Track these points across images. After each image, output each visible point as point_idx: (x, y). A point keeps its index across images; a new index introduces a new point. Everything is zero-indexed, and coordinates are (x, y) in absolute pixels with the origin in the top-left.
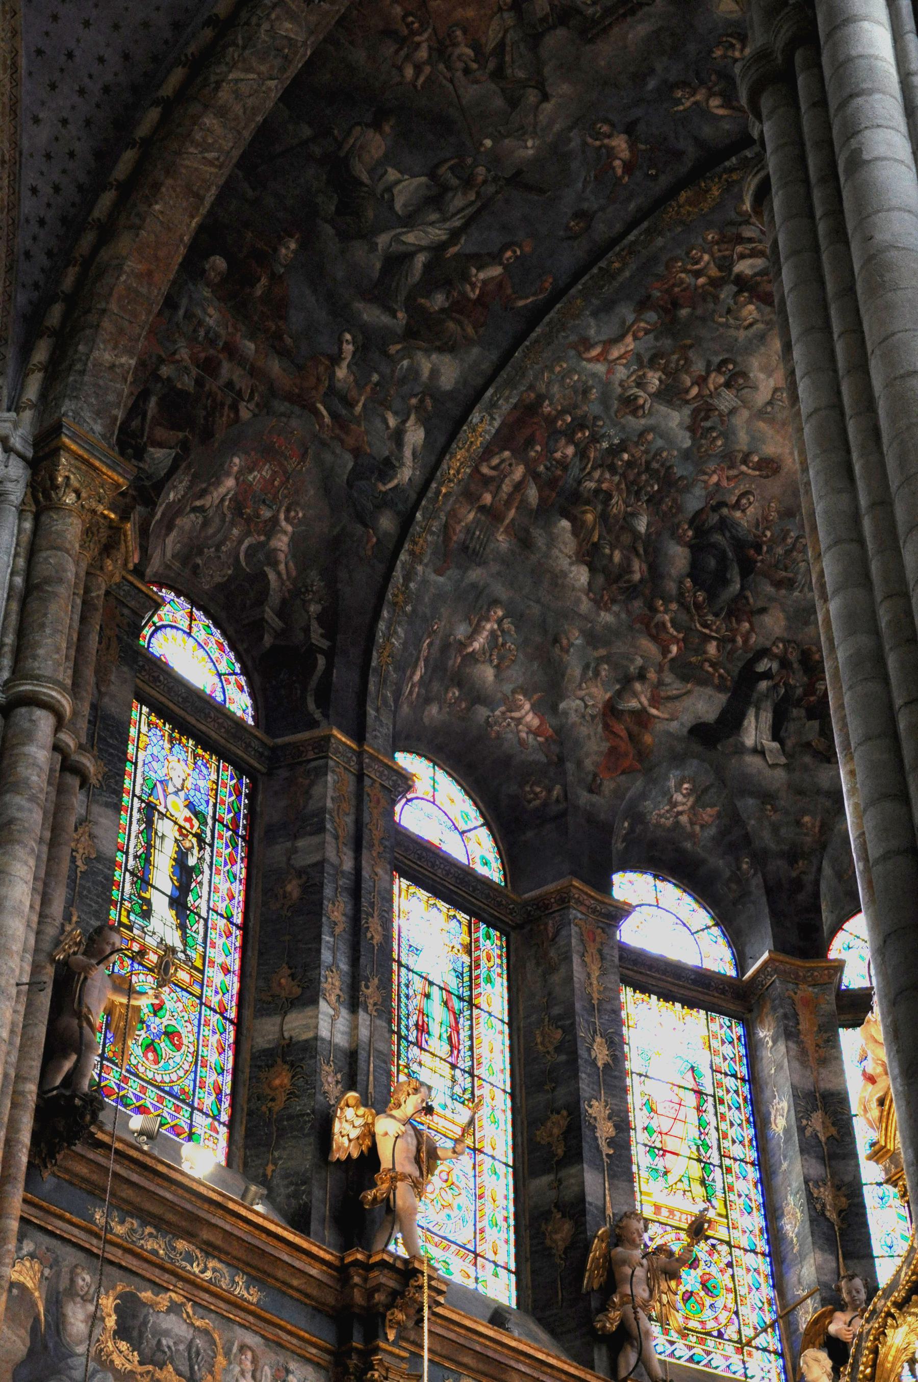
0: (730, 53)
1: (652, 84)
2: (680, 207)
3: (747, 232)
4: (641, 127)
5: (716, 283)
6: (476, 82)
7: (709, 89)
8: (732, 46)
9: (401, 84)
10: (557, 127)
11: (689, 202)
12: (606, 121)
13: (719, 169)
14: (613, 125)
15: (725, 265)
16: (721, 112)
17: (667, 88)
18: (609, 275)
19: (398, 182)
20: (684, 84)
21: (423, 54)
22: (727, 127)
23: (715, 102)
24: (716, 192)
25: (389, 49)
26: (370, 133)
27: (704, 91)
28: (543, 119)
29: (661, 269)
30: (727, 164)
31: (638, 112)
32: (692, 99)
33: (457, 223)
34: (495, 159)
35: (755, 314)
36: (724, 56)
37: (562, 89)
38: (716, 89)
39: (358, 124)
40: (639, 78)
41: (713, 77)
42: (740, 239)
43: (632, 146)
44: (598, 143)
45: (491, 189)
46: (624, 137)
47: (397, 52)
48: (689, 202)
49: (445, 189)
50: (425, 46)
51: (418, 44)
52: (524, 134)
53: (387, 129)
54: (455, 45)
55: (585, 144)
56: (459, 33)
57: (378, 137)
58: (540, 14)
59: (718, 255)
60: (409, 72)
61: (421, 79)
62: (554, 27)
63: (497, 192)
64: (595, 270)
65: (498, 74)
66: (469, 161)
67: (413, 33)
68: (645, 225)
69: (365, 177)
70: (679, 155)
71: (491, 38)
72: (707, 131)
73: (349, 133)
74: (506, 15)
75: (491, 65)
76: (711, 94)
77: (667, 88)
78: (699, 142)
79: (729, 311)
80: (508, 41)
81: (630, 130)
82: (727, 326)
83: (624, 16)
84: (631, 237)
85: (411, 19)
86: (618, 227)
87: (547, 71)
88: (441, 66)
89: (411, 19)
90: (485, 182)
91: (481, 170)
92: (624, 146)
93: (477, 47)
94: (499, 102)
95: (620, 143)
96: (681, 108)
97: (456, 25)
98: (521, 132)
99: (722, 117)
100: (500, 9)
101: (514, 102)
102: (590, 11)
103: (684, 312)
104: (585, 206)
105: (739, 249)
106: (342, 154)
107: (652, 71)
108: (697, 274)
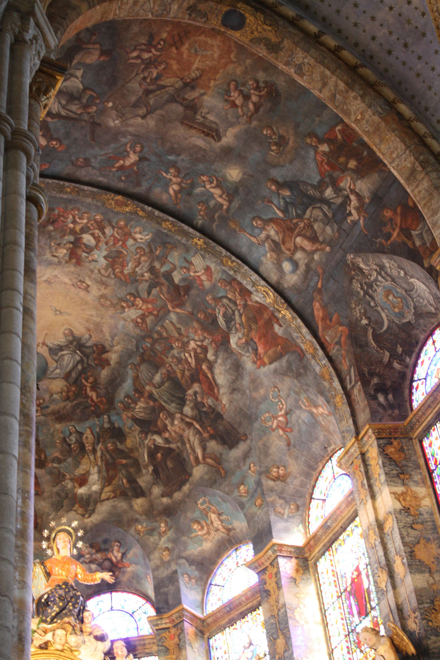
0: (206, 183)
1: (172, 158)
2: (112, 199)
3: (108, 231)
4: (146, 163)
5: (73, 232)
6: (140, 85)
7: (182, 182)
8: (212, 183)
9: (127, 53)
10: (130, 129)
11: (117, 202)
12: (142, 147)
13: (141, 205)
14: (141, 151)
15: (84, 230)
16: (171, 192)
17: (174, 165)
18: (62, 190)
19: (77, 77)
20: (178, 171)
21: (146, 56)
22: (164, 197)
23: (176, 187)
24: (127, 209)
25: (143, 40)
26: (98, 52)
27: (179, 180)
28: (132, 121)
29: (70, 207)
30: (146, 207)
31: (153, 158)
32: (172, 177)
33: (63, 113)
34: (103, 112)
35: (61, 255)
36: (204, 182)
37: (151, 122)
38: (183, 185)
39: (101, 45)
40: (172, 151)
41: (189, 181)
42: (102, 229)
43: (133, 164)
44: (129, 149)
45: (86, 117)
46: (137, 158)
47: (144, 44)
48: (117, 202)
49: (79, 99)
50: (151, 55)
51: (151, 52)
52: (121, 117)
53: (102, 58)
54: (156, 68)
55: (126, 144)
56: (163, 66)
57: (97, 57)
58: (186, 96)
59: (89, 225)
60: (135, 54)
61: (133, 61)
62: (182, 104)
63: (85, 121)
64: (62, 183)
65: (148, 92)
66: (98, 101)
67: (155, 47)
68: (95, 190)
69: (75, 62)
70: (139, 184)
71: (166, 81)
72: (157, 190)
73: (94, 43)
74: (180, 83)
75: (152, 87)
76: (179, 184)
77: (174, 165)
78: (149, 190)
79: (59, 244)
80: (167, 89)
81: (142, 159)
82: (50, 247)
83: (204, 132)
84: (86, 188)
85: (162, 43)
86: (87, 179)
87: (159, 112)
88: (143, 66)
89: (162, 43)
90: (89, 113)
91: (94, 108)
92: (132, 161)
93: (159, 77)
94: (133, 99)
95: (133, 158)
96: (164, 174)
97: (167, 64)
98: (121, 115)
99: (169, 193)
100: (182, 79)
101: (135, 105)
102: (198, 117)
103: (51, 228)
104: (93, 160)
105: (97, 231)
106: (84, 46)
107: (179, 155)
108: (74, 222)
